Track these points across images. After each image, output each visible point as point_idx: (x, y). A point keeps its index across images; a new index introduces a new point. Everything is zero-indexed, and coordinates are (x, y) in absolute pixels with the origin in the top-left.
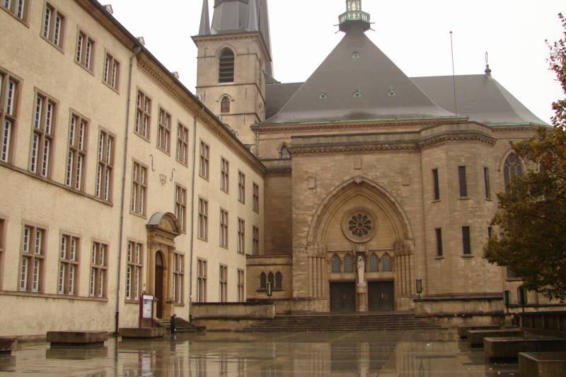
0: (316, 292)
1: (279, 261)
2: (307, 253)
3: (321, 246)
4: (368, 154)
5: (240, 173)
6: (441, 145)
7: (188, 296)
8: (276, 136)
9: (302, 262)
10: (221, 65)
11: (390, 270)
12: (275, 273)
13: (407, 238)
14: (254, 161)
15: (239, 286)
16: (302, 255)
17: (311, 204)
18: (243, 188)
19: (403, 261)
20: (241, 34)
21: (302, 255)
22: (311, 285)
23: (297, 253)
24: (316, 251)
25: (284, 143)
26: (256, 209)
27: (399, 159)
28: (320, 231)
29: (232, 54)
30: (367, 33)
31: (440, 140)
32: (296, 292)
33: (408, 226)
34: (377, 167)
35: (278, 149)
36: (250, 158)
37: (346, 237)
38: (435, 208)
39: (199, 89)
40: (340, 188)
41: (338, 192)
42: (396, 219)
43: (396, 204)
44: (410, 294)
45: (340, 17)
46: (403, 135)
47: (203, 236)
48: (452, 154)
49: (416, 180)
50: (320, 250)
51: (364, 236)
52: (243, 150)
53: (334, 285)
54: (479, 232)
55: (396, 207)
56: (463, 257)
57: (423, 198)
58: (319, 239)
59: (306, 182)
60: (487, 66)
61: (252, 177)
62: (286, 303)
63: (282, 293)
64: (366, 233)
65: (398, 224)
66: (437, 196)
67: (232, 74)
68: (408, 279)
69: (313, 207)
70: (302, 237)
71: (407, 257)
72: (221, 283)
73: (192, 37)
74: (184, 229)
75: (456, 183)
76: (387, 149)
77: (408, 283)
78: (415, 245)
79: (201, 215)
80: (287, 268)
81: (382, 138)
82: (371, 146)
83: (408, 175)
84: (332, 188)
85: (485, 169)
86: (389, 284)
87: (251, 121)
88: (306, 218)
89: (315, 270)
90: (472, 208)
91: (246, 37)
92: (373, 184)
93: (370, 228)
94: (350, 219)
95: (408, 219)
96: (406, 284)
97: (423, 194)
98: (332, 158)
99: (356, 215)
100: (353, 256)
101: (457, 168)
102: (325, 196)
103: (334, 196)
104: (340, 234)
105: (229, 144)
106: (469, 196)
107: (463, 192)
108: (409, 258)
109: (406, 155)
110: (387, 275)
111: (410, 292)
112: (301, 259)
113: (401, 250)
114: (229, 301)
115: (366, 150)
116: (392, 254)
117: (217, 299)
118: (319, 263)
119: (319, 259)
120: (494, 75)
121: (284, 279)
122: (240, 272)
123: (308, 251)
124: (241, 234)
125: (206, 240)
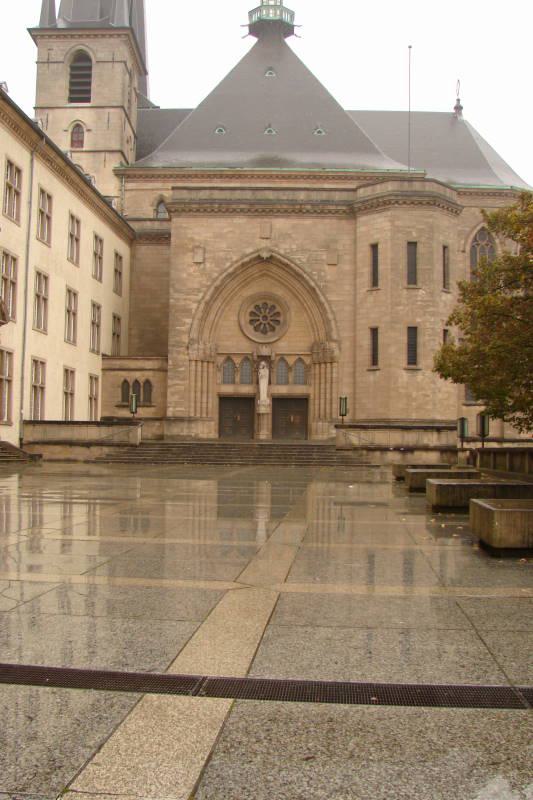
0: (198, 409)
1: (149, 364)
2: (188, 354)
3: (208, 345)
4: (282, 217)
5: (96, 237)
6: (384, 210)
7: (18, 411)
8: (150, 186)
10: (72, 76)
11: (305, 383)
12: (142, 381)
13: (329, 338)
14: (116, 220)
15: (91, 399)
16: (182, 357)
17: (196, 286)
18: (100, 258)
19: (323, 371)
20: (103, 30)
21: (182, 357)
23: (175, 355)
24: (201, 352)
25: (161, 196)
26: (118, 290)
27: (323, 227)
28: (208, 324)
29: (90, 60)
30: (289, 41)
31: (385, 203)
32: (171, 409)
33: (333, 323)
34: (291, 237)
35: (152, 205)
36: (111, 215)
37: (242, 331)
38: (371, 299)
39: (39, 110)
40: (240, 263)
41: (236, 269)
42: (315, 311)
43: (317, 289)
44: (331, 417)
45: (251, 13)
46: (333, 193)
47: (41, 326)
48: (397, 223)
49: (347, 257)
50: (208, 352)
51: (269, 334)
52: (101, 204)
53: (225, 400)
55: (317, 295)
56: (405, 369)
57: (355, 285)
58: (206, 335)
59: (190, 254)
60: (458, 100)
61: (114, 243)
62: (157, 424)
63: (152, 410)
64: (273, 329)
65: (318, 318)
66: (375, 282)
67: (89, 92)
68: (328, 396)
69: (199, 291)
71: (328, 365)
72: (66, 393)
73: (29, 30)
74: (14, 316)
75: (403, 265)
76: (308, 211)
77: (328, 402)
78: (340, 349)
79: (38, 296)
80: (160, 375)
81: (302, 196)
82: (285, 207)
83: (336, 250)
84: (228, 264)
85: (445, 248)
86: (302, 402)
87: (114, 162)
89: (199, 379)
90: (421, 301)
91: (111, 36)
92: (286, 261)
93: (278, 322)
94: (252, 309)
95: (333, 312)
96: (325, 404)
97: (355, 279)
98: (229, 220)
99: (260, 303)
100: (254, 361)
101: (405, 244)
102: (216, 275)
103: (230, 275)
104: (237, 328)
105: (81, 195)
106: (419, 284)
107: (412, 278)
108: (332, 368)
109: (334, 221)
110: (299, 390)
111: (331, 414)
112: (181, 363)
113: (321, 355)
114: (76, 419)
115: (278, 211)
116: (308, 361)
117: (59, 417)
118: (205, 369)
119: (205, 364)
120: (466, 115)
121: (154, 390)
122: (93, 378)
123: (190, 352)
124: (96, 325)
125: (45, 332)
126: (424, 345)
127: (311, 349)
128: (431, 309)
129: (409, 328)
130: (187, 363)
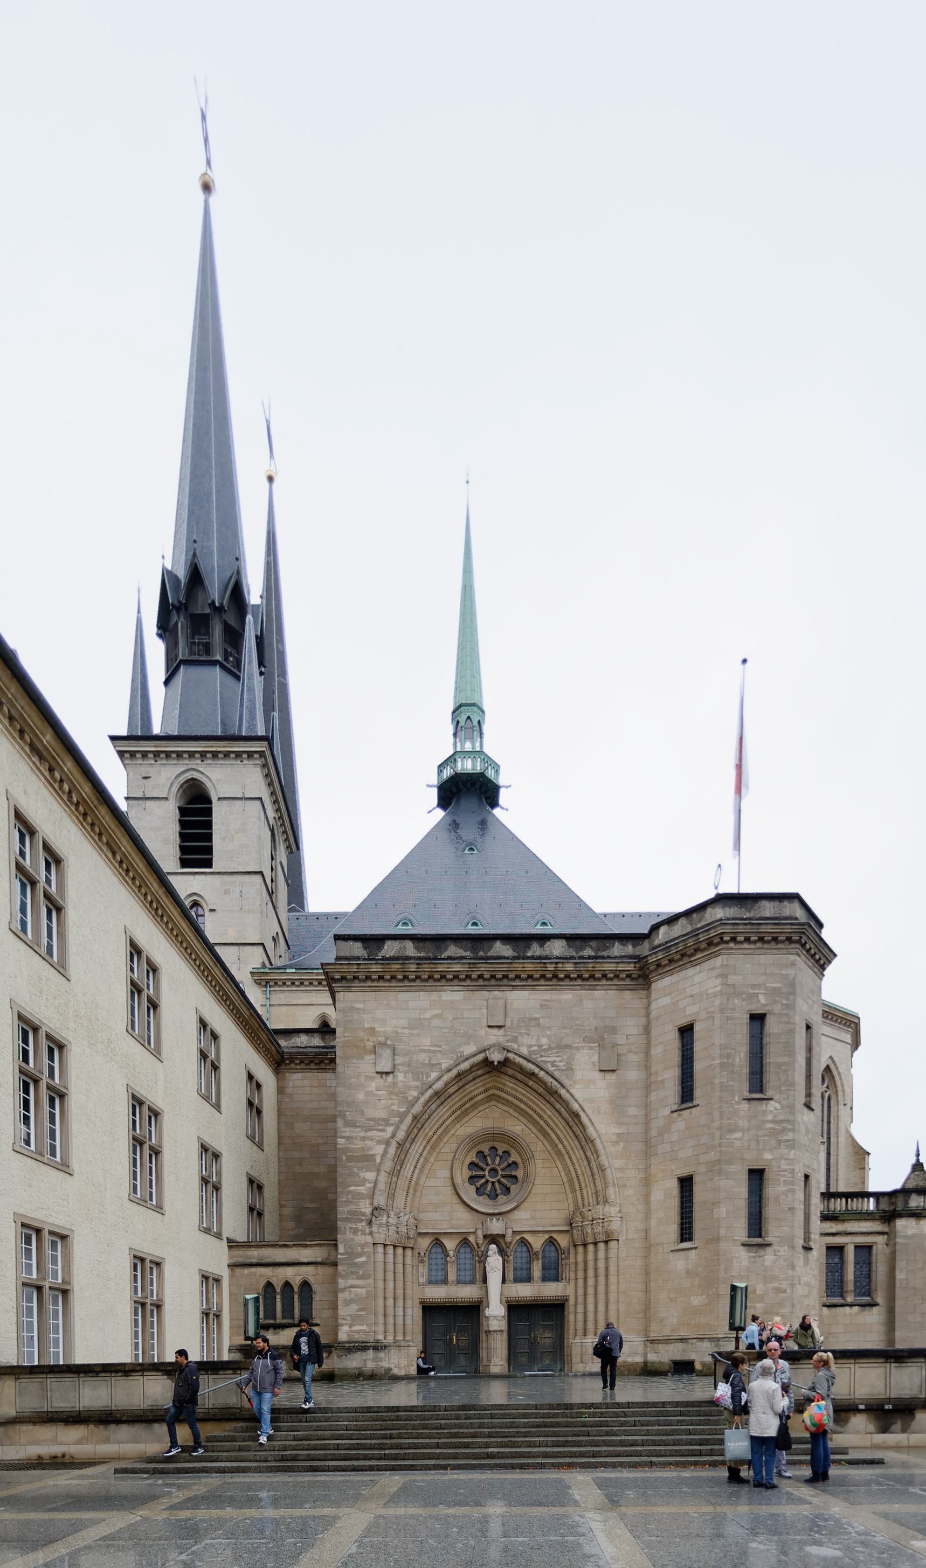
2: (371, 1233)
3: (404, 1219)
9: (360, 1255)
16: (360, 1239)
21: (360, 1239)
22: (381, 1311)
23: (349, 1235)
24: (393, 1229)
28: (402, 1183)
38: (680, 1124)
40: (455, 1072)
50: (403, 1230)
54: (785, 1182)
69: (386, 1122)
70: (360, 1196)
84: (434, 1075)
88: (370, 1149)
89: (390, 1275)
92: (531, 1067)
102: (415, 1094)
103: (437, 1094)
123: (375, 1229)
126: (777, 1199)
128: (790, 1136)
129: (751, 1172)
130: (369, 1249)
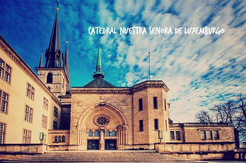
127: (117, 128)
